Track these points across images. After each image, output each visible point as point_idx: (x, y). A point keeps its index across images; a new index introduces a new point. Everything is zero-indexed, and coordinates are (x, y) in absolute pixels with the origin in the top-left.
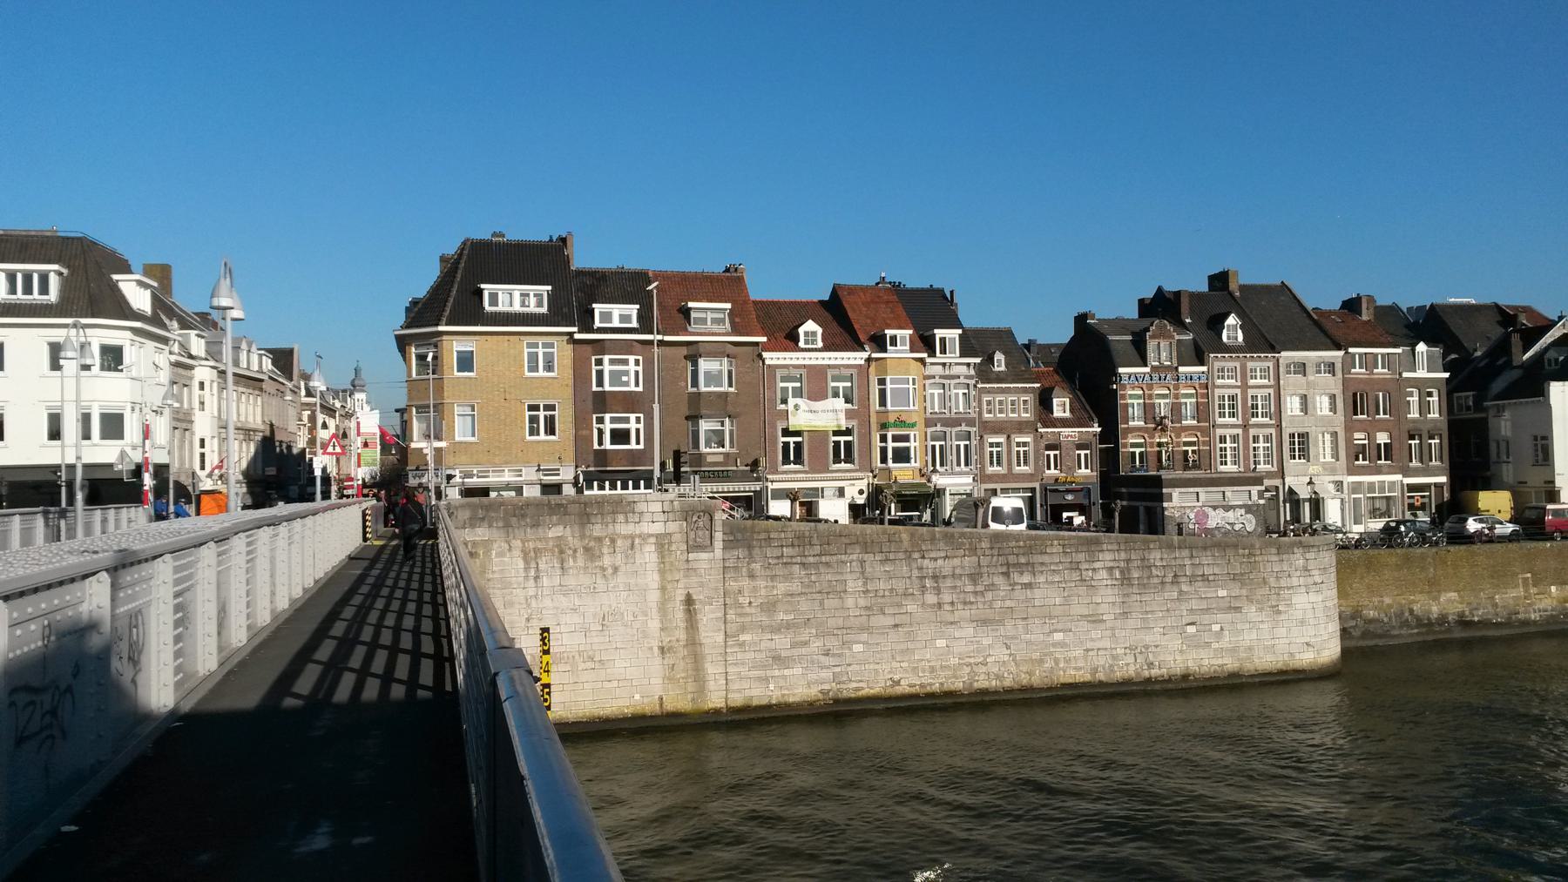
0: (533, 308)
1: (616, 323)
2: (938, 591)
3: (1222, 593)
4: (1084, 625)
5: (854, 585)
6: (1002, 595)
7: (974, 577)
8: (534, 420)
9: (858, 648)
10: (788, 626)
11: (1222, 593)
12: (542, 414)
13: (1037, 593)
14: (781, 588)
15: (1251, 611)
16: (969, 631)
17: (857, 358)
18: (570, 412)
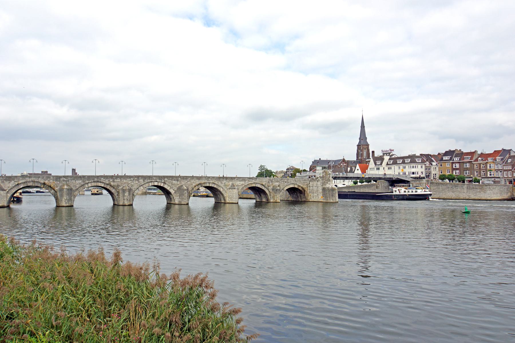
0: (448, 159)
1: (456, 160)
2: (448, 189)
3: (479, 190)
4: (462, 193)
5: (441, 188)
6: (455, 189)
7: (452, 187)
8: (448, 171)
9: (441, 194)
10: (435, 191)
11: (479, 190)
12: (448, 171)
13: (458, 189)
14: (435, 188)
15: (482, 192)
16: (451, 193)
17: (485, 162)
18: (451, 170)
